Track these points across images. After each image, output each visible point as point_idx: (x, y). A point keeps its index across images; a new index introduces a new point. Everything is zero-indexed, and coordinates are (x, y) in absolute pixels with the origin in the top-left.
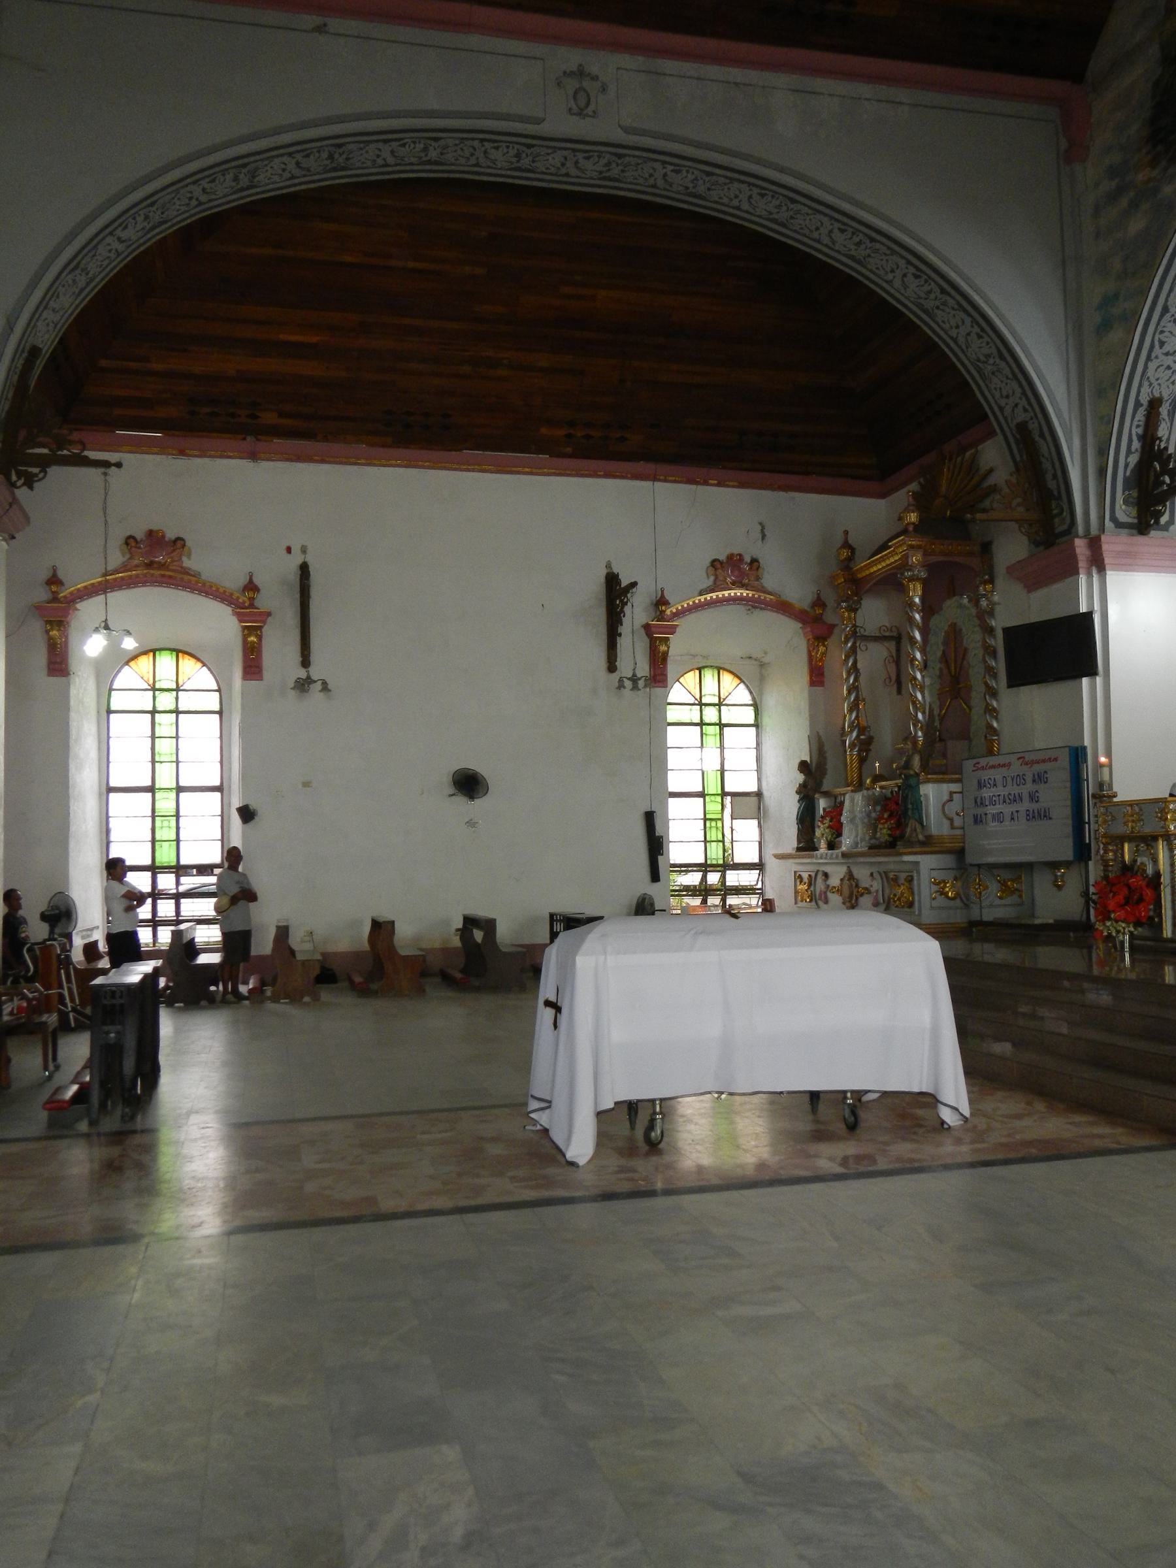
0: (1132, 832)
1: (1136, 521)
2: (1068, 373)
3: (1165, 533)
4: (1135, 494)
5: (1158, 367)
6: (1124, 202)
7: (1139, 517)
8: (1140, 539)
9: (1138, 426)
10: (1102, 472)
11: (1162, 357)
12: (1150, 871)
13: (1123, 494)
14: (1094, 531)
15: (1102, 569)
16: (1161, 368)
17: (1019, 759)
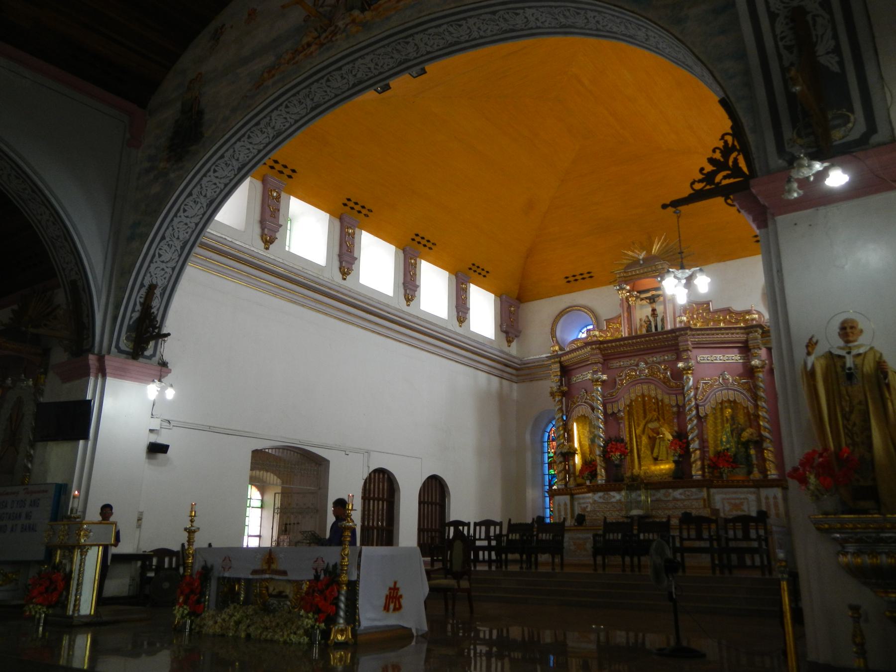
0: (61, 543)
1: (132, 351)
2: (106, 258)
3: (147, 361)
4: (134, 335)
5: (157, 268)
7: (134, 349)
8: (131, 361)
9: (141, 297)
10: (115, 318)
11: (159, 262)
12: (68, 569)
13: (126, 333)
14: (104, 352)
15: (104, 376)
16: (158, 268)
17: (24, 489)
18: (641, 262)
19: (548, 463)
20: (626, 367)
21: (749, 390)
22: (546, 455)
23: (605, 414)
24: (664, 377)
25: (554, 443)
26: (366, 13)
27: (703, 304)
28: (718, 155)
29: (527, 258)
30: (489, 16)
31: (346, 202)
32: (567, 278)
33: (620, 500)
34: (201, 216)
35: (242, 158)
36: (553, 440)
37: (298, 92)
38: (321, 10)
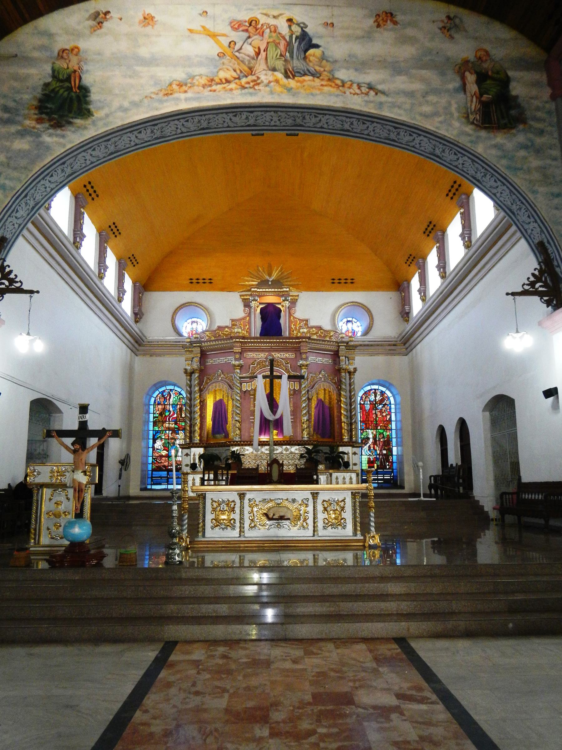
6: (13, 129)
18: (270, 283)
19: (153, 422)
20: (258, 359)
21: (335, 383)
22: (151, 416)
23: (241, 390)
24: (286, 369)
25: (160, 407)
26: (290, 80)
27: (303, 320)
28: (537, 273)
29: (166, 257)
30: (391, 128)
31: (87, 184)
32: (191, 279)
33: (252, 453)
34: (56, 184)
35: (121, 146)
36: (159, 404)
37: (205, 115)
38: (237, 54)
